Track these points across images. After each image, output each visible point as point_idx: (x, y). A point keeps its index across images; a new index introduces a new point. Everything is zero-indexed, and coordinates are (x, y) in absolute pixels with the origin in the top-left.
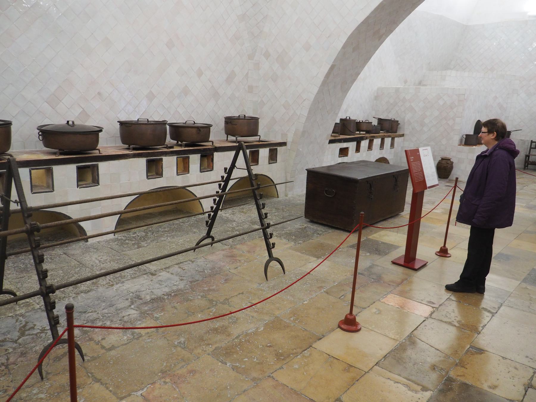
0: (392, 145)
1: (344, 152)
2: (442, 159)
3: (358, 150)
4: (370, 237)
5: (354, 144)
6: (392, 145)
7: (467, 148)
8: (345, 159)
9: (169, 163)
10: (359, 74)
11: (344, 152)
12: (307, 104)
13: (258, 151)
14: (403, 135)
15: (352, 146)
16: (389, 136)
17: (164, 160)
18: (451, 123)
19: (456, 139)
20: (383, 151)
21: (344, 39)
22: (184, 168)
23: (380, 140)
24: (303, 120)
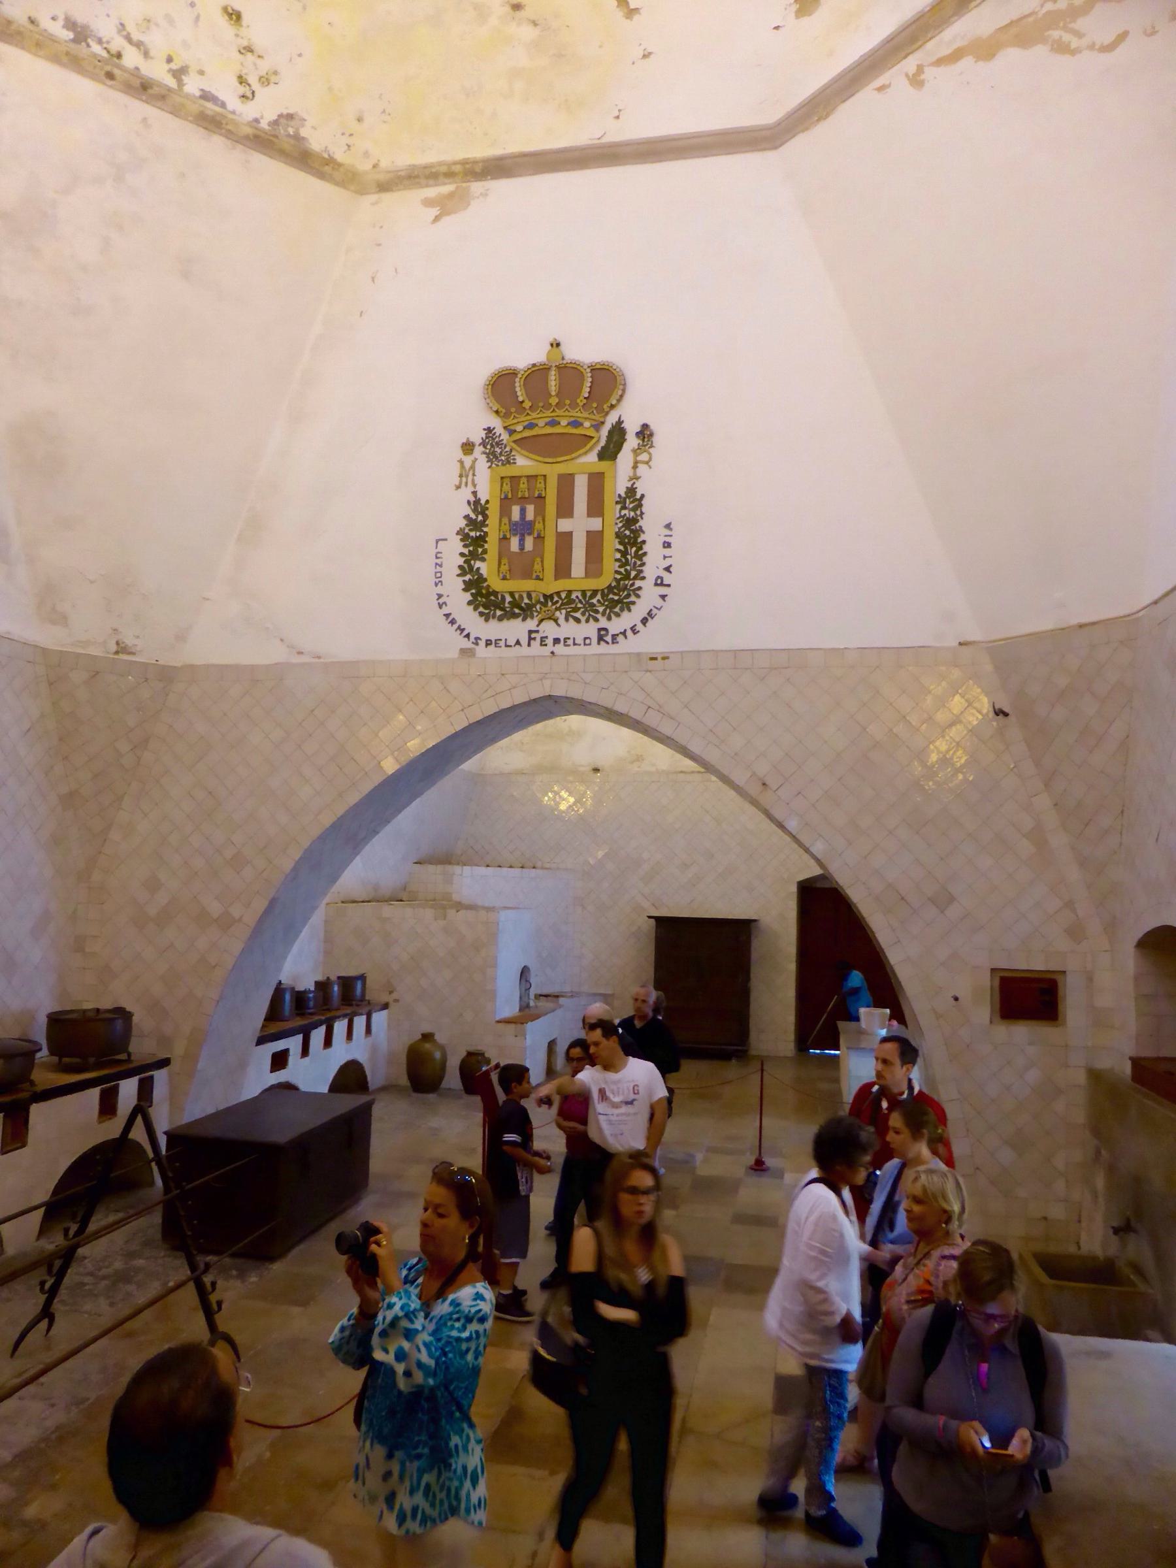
1: (279, 1061)
3: (305, 1052)
5: (300, 1037)
8: (281, 1076)
11: (279, 1061)
13: (117, 1086)
15: (293, 1044)
21: (296, 854)
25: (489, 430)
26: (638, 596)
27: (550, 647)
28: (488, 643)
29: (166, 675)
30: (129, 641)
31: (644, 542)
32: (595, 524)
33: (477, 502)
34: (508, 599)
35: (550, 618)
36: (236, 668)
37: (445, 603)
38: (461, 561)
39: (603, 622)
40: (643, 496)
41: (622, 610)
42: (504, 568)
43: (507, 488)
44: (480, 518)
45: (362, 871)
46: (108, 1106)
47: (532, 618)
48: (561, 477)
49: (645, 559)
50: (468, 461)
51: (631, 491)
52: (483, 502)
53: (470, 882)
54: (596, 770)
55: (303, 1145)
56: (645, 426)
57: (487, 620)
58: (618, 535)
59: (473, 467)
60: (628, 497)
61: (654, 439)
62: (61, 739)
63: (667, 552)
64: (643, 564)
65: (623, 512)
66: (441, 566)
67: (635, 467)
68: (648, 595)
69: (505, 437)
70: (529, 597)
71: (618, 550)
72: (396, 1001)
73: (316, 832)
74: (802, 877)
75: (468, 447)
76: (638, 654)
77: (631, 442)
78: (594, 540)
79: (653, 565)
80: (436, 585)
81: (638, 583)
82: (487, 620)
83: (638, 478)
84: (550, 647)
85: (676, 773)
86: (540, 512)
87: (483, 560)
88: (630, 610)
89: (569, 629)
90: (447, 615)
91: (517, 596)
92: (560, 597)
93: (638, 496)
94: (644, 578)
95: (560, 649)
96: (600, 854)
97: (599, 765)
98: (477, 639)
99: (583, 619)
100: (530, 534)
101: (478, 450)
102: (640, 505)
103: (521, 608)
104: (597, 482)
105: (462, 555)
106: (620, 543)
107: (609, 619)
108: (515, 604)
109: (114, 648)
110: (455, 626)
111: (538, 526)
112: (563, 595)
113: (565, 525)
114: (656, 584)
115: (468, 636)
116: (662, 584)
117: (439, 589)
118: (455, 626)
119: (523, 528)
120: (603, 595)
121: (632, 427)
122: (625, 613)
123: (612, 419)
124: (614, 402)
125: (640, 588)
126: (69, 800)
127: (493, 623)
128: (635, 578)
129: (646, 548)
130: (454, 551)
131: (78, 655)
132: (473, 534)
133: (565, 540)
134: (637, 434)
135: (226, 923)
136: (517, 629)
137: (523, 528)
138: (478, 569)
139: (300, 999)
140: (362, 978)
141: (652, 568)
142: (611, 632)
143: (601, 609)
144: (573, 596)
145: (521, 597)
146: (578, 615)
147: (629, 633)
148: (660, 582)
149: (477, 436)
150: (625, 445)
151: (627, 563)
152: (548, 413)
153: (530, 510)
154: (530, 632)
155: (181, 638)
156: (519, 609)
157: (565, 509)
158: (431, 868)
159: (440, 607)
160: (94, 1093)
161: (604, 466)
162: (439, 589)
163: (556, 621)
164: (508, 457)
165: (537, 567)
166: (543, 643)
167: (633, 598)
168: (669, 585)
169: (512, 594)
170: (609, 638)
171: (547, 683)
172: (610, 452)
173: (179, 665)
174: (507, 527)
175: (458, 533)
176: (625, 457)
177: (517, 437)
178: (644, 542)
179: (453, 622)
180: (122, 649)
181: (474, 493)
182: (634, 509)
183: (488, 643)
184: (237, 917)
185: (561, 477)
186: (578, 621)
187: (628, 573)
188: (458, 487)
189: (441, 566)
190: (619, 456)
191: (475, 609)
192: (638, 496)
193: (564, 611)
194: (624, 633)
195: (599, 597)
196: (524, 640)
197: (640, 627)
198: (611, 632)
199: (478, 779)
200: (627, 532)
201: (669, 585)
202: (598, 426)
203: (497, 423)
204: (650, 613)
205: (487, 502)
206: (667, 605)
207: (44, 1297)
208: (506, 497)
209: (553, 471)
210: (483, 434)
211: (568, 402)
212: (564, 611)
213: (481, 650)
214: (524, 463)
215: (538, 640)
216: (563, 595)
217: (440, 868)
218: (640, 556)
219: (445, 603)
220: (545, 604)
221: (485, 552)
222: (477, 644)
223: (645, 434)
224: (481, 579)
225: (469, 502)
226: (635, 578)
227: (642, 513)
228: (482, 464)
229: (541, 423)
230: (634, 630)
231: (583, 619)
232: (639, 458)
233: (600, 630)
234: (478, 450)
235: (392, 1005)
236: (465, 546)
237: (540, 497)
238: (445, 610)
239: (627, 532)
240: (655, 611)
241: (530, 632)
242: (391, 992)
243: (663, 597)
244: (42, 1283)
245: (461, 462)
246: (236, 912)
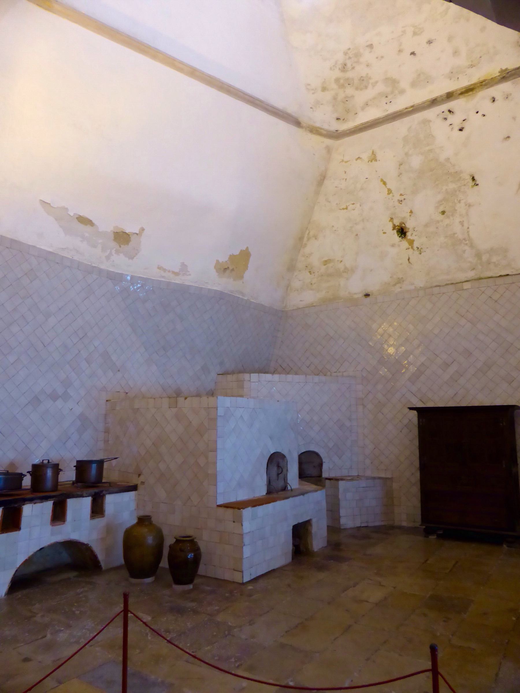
14: (134, 488)
54: (367, 295)
72: (143, 483)
85: (431, 287)
97: (368, 291)
158: (229, 377)
242: (139, 475)
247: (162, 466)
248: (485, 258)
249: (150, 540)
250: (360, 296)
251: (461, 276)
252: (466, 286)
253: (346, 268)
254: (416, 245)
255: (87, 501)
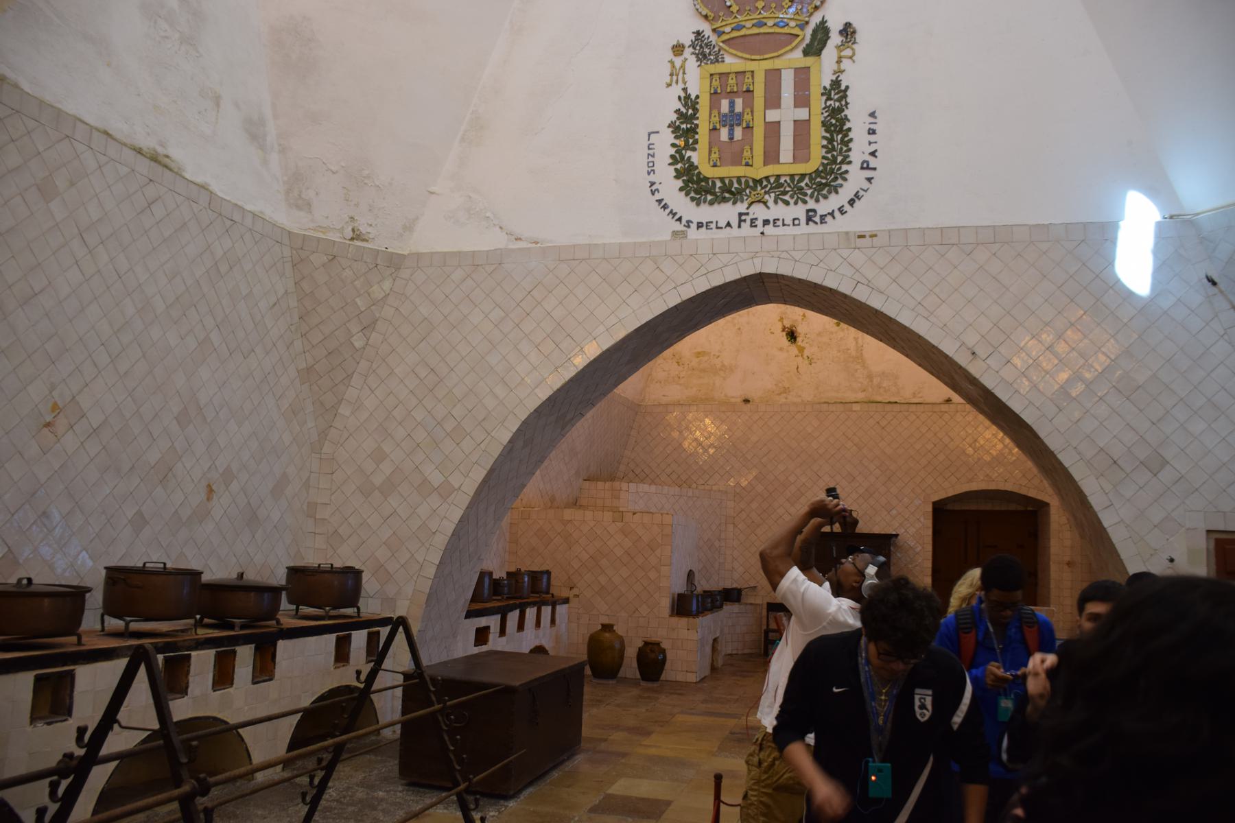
0: (553, 621)
1: (482, 636)
2: (646, 643)
4: (610, 791)
5: (498, 617)
6: (553, 621)
7: (683, 622)
9: (202, 662)
10: (524, 486)
12: (441, 541)
13: (349, 636)
15: (493, 622)
16: (545, 603)
17: (193, 660)
18: (653, 575)
19: (665, 604)
20: (541, 632)
22: (223, 677)
23: (535, 610)
24: (431, 571)
25: (698, 33)
26: (845, 180)
27: (760, 228)
28: (700, 225)
29: (395, 262)
30: (363, 229)
31: (849, 129)
32: (802, 114)
33: (688, 97)
34: (719, 184)
35: (759, 201)
36: (459, 254)
37: (657, 190)
38: (673, 151)
39: (811, 204)
40: (847, 87)
41: (829, 192)
42: (715, 156)
43: (716, 83)
44: (690, 111)
45: (535, 488)
46: (342, 655)
47: (742, 201)
48: (767, 72)
49: (851, 145)
50: (678, 61)
51: (836, 83)
52: (693, 97)
53: (635, 496)
55: (537, 689)
56: (848, 25)
57: (698, 204)
58: (824, 124)
59: (683, 67)
60: (832, 89)
61: (857, 36)
62: (301, 318)
63: (872, 138)
64: (850, 150)
65: (829, 103)
66: (653, 156)
67: (839, 62)
68: (855, 178)
69: (713, 38)
70: (739, 182)
71: (824, 138)
73: (533, 404)
74: (936, 498)
75: (678, 49)
76: (847, 233)
77: (835, 39)
78: (801, 128)
79: (859, 150)
80: (649, 173)
81: (844, 167)
82: (698, 204)
83: (842, 72)
84: (760, 228)
86: (749, 104)
87: (694, 150)
88: (837, 192)
89: (777, 211)
90: (660, 201)
91: (727, 181)
92: (769, 181)
93: (843, 87)
94: (850, 162)
95: (769, 229)
96: (751, 477)
98: (689, 222)
99: (792, 202)
100: (738, 125)
101: (688, 52)
102: (845, 96)
103: (730, 192)
104: (802, 76)
105: (673, 145)
106: (826, 131)
107: (817, 201)
108: (726, 189)
109: (349, 234)
110: (668, 211)
111: (747, 117)
112: (772, 180)
113: (772, 115)
114: (862, 168)
115: (680, 219)
116: (868, 168)
117: (652, 178)
118: (668, 211)
119: (732, 120)
120: (811, 179)
121: (835, 26)
122: (833, 196)
123: (816, 19)
124: (818, 4)
125: (847, 172)
126: (307, 374)
127: (705, 208)
128: (842, 162)
129: (851, 135)
130: (665, 143)
131: (319, 240)
132: (684, 126)
133: (773, 130)
134: (841, 32)
135: (445, 492)
136: (727, 212)
137: (732, 120)
138: (689, 158)
139: (496, 584)
140: (548, 573)
141: (858, 153)
142: (820, 212)
143: (809, 192)
144: (782, 180)
145: (731, 183)
146: (787, 198)
147: (837, 214)
148: (865, 166)
149: (687, 39)
150: (829, 42)
151: (833, 149)
152: (755, 16)
153: (739, 103)
154: (740, 214)
155: (409, 228)
156: (730, 192)
157: (773, 101)
158: (600, 485)
159: (653, 194)
160: (332, 637)
161: (810, 61)
162: (652, 178)
163: (765, 203)
164: (717, 54)
165: (747, 154)
166: (753, 224)
167: (840, 181)
168: (875, 169)
169: (722, 179)
170: (817, 219)
171: (757, 261)
172: (815, 47)
173: (405, 253)
174: (717, 119)
175: (669, 126)
176: (830, 52)
177: (725, 37)
178: (849, 129)
179: (665, 207)
180: (357, 236)
181: (685, 90)
182: (839, 100)
183: (700, 225)
184: (456, 486)
185: (767, 72)
186: (787, 203)
187: (835, 158)
188: (669, 85)
189: (653, 156)
190: (824, 52)
191: (687, 195)
192: (843, 87)
193: (773, 195)
194: (832, 214)
195: (807, 180)
196: (735, 223)
197: (847, 207)
198: (820, 212)
199: (635, 408)
200: (833, 121)
201: (875, 169)
202: (803, 25)
203: (706, 28)
204: (857, 195)
205: (697, 97)
206: (872, 187)
207: (306, 809)
208: (716, 93)
209: (760, 68)
210: (693, 37)
211: (773, 5)
212: (773, 195)
213: (693, 233)
214: (731, 62)
215: (748, 222)
216: (772, 180)
217: (608, 484)
218: (846, 143)
219: (657, 190)
220: (754, 188)
221: (696, 142)
222: (689, 227)
223: (848, 32)
224: (692, 167)
225: (679, 98)
226: (842, 162)
227: (847, 104)
228: (692, 62)
229: (748, 24)
230: (841, 211)
231: (792, 202)
232: (844, 53)
233: (808, 211)
234: (688, 52)
235: (574, 602)
236: (676, 137)
237: (748, 91)
238: (658, 196)
239: (833, 121)
240: (861, 193)
241: (740, 214)
243: (869, 180)
244: (304, 795)
245: (671, 62)
246: (455, 480)
247: (603, 580)
248: (876, 381)
249: (617, 646)
250: (739, 400)
251: (851, 396)
252: (856, 407)
253: (723, 365)
254: (806, 353)
255: (549, 608)
